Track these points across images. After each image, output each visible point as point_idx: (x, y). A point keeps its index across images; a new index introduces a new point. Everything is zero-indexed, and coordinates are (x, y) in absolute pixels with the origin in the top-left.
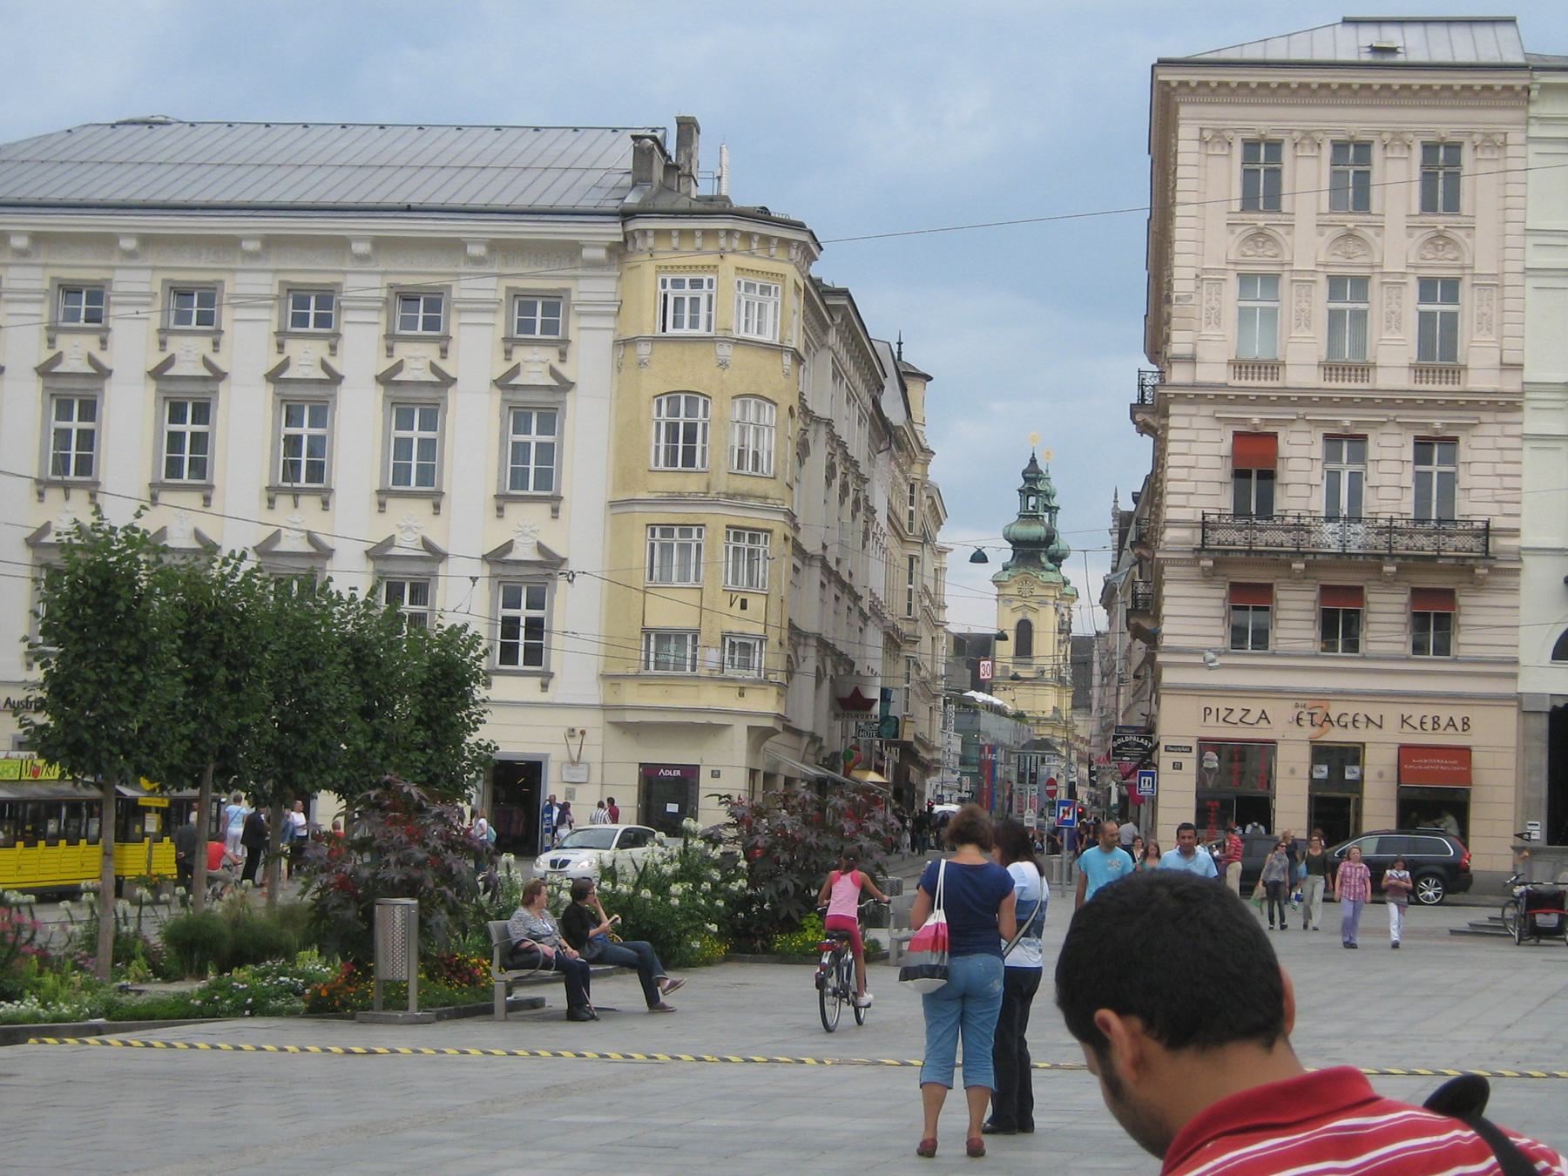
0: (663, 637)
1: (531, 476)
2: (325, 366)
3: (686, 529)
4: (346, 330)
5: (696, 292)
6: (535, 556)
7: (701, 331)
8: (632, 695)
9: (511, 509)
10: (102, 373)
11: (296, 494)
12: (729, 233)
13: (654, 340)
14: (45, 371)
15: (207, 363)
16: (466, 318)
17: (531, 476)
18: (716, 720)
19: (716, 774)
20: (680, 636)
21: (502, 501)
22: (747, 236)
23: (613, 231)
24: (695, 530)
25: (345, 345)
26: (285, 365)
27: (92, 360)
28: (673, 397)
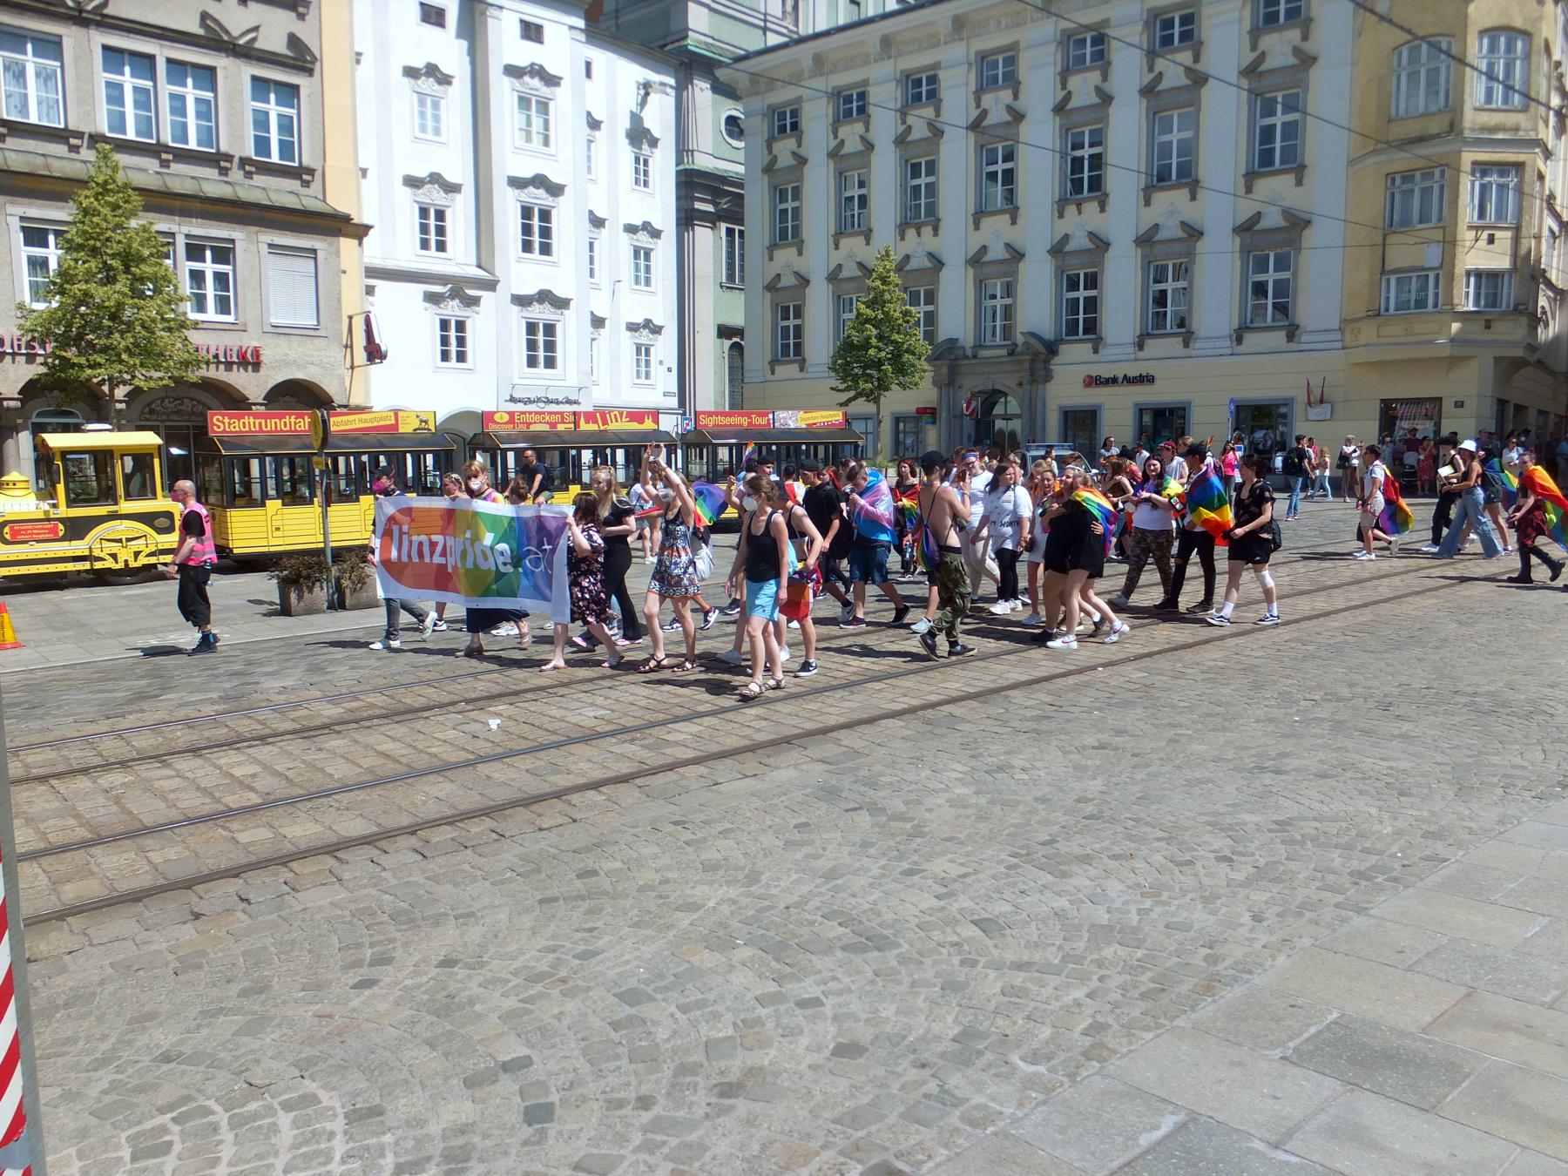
1: (1274, 151)
6: (1282, 223)
17: (1274, 151)
19: (1459, 405)
21: (1250, 177)
24: (1437, 172)
25: (1116, 72)
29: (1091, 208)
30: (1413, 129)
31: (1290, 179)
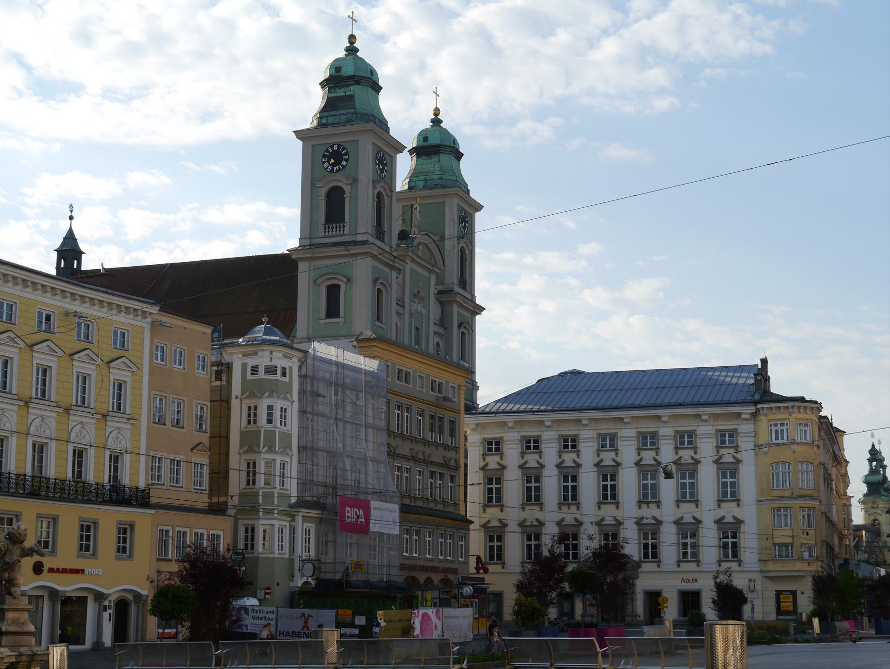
0: (781, 545)
1: (729, 493)
2: (655, 459)
3: (785, 509)
4: (661, 447)
5: (782, 428)
7: (785, 441)
8: (770, 566)
9: (723, 505)
10: (579, 466)
11: (648, 503)
12: (793, 407)
13: (770, 445)
14: (559, 466)
15: (614, 460)
16: (702, 440)
17: (729, 493)
18: (801, 574)
19: (803, 593)
20: (787, 546)
21: (719, 502)
22: (799, 407)
23: (752, 409)
26: (641, 460)
27: (574, 461)
28: (777, 463)
29: (653, 506)
30: (780, 493)
31: (734, 504)
